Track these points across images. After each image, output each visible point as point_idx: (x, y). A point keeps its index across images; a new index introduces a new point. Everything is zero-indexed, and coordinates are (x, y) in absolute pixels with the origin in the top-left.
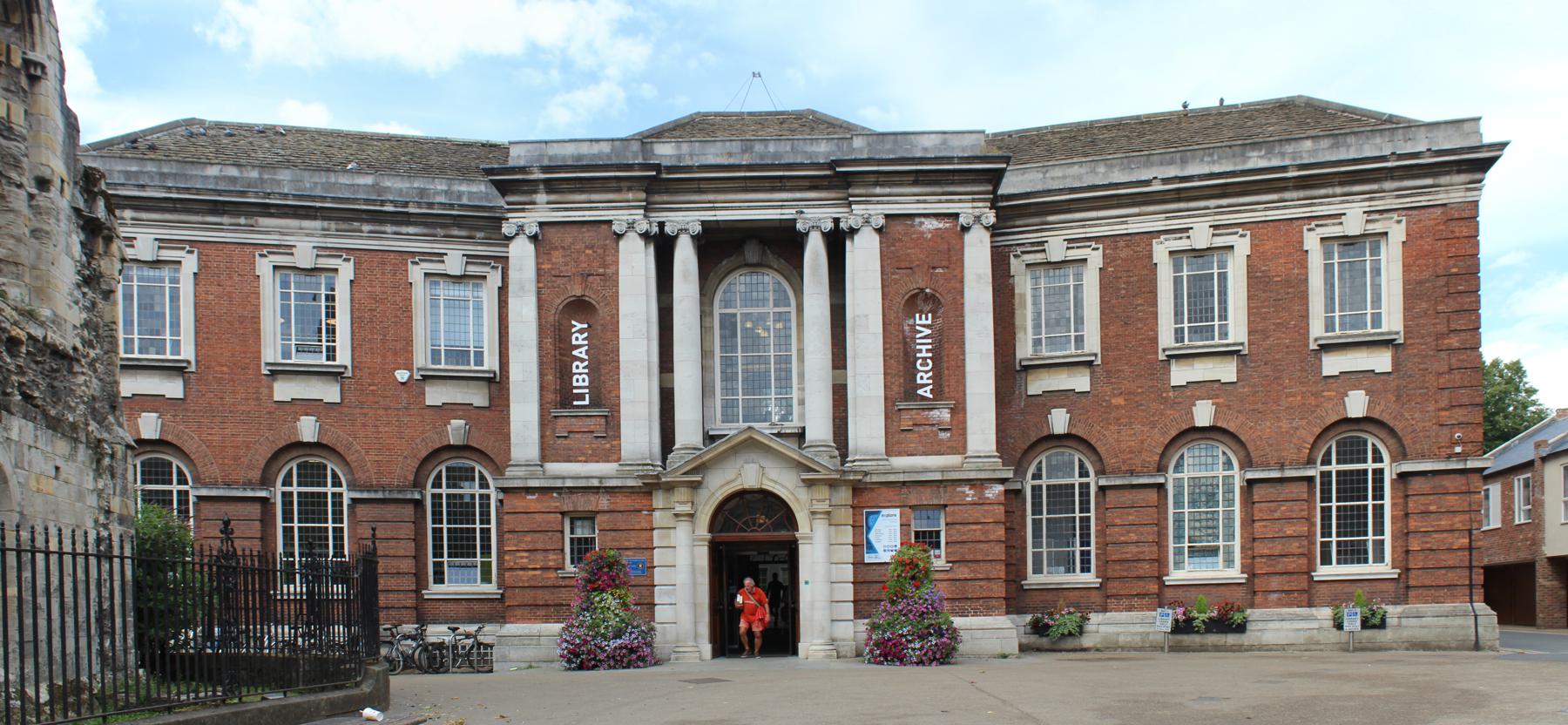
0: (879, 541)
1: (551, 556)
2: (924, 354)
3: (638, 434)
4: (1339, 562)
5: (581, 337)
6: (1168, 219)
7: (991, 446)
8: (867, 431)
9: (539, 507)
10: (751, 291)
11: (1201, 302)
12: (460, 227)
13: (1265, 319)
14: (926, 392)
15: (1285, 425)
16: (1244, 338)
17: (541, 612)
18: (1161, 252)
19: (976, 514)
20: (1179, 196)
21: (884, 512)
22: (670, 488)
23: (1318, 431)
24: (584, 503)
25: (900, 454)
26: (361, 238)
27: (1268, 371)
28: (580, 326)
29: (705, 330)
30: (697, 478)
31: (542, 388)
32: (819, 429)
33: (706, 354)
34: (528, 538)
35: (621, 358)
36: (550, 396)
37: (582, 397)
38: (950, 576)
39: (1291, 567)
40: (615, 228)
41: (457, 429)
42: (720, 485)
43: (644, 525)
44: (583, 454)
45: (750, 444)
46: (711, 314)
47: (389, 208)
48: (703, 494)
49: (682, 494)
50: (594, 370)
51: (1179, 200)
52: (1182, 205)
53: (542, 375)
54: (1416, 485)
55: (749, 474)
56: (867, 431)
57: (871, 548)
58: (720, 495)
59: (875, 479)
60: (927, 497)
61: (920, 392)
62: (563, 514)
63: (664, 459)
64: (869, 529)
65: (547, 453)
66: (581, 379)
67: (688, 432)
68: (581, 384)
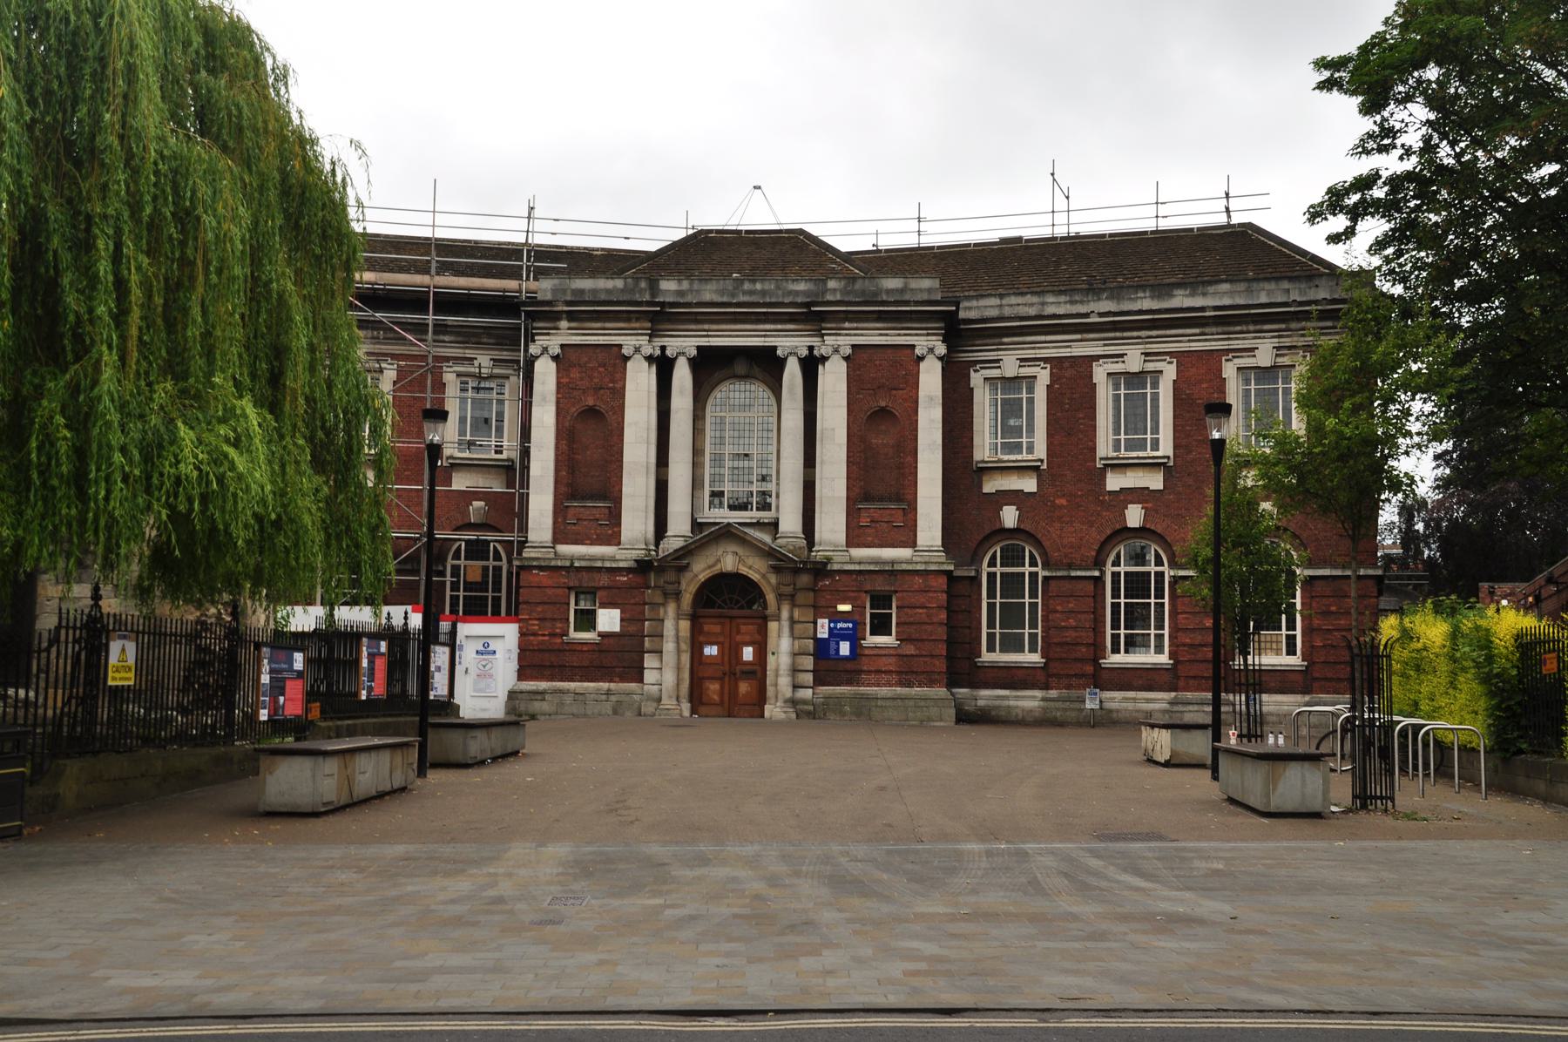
3: (636, 522)
9: (550, 582)
10: (738, 398)
11: (1135, 417)
16: (1170, 453)
17: (547, 672)
18: (1100, 373)
19: (922, 599)
20: (1114, 327)
24: (586, 581)
25: (858, 546)
31: (556, 482)
32: (790, 522)
34: (539, 609)
38: (900, 652)
42: (701, 569)
48: (688, 575)
49: (671, 576)
51: (1115, 330)
52: (1118, 334)
54: (1319, 585)
55: (728, 560)
56: (832, 526)
58: (702, 577)
60: (880, 585)
62: (570, 588)
63: (657, 545)
65: (560, 536)
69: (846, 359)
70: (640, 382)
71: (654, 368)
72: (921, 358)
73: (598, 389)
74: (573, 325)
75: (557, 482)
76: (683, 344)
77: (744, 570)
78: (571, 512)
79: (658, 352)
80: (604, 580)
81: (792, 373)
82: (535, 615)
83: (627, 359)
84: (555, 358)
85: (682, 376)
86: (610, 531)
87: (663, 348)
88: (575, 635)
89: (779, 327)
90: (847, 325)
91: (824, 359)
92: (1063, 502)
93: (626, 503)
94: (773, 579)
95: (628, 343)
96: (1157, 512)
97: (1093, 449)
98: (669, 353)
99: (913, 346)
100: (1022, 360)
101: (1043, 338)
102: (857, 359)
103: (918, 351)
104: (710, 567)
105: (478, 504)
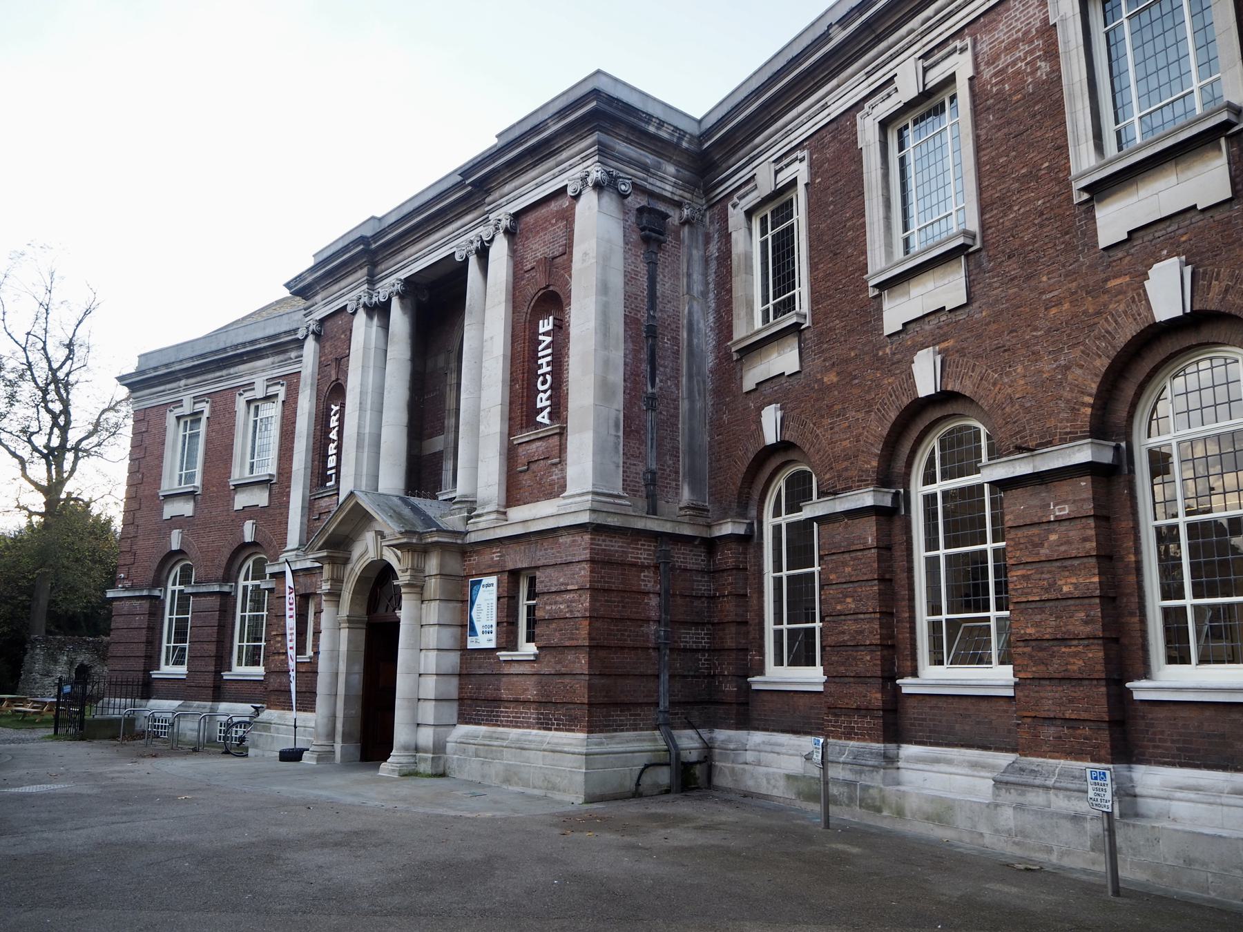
4: (1203, 660)
6: (869, 75)
13: (1003, 176)
15: (1047, 366)
23: (1102, 364)
26: (290, 364)
27: (1012, 268)
36: (315, 481)
39: (1076, 665)
71: (376, 319)
92: (831, 378)
96: (962, 352)
97: (864, 268)
99: (563, 190)
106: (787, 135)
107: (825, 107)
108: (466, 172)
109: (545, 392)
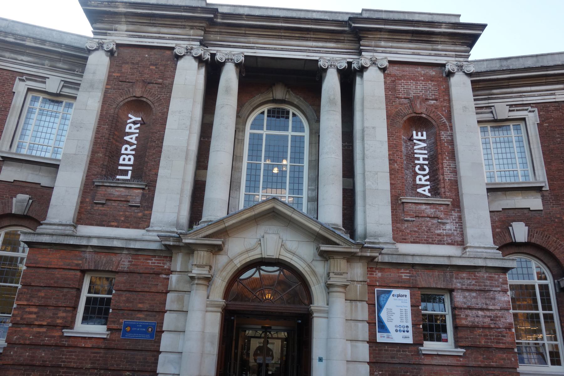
0: (391, 320)
1: (61, 314)
2: (421, 162)
3: (169, 206)
5: (134, 127)
7: (489, 241)
8: (376, 217)
9: (61, 264)
12: (64, 62)
14: (425, 191)
21: (395, 292)
22: (190, 249)
25: (404, 241)
28: (134, 119)
29: (238, 141)
30: (219, 242)
32: (331, 213)
33: (236, 158)
35: (165, 143)
37: (125, 173)
40: (176, 51)
41: (22, 201)
43: (160, 288)
44: (116, 220)
45: (273, 215)
46: (244, 131)
47: (11, 39)
48: (222, 259)
49: (202, 256)
50: (139, 155)
53: (94, 152)
57: (383, 328)
58: (238, 263)
59: (387, 259)
61: (420, 190)
64: (380, 308)
65: (84, 215)
66: (127, 158)
67: (215, 207)
68: (126, 162)
69: (383, 70)
70: (189, 78)
71: (203, 71)
72: (450, 74)
73: (146, 83)
74: (131, 27)
75: (92, 162)
76: (231, 53)
77: (287, 257)
78: (101, 190)
79: (207, 57)
80: (125, 263)
81: (331, 85)
82: (35, 301)
83: (178, 57)
84: (111, 53)
85: (229, 78)
86: (140, 215)
87: (213, 55)
88: (83, 329)
89: (320, 44)
90: (383, 43)
91: (363, 69)
93: (161, 184)
94: (320, 268)
95: (180, 47)
98: (218, 57)
99: (444, 65)
100: (511, 106)
101: (528, 89)
102: (392, 71)
103: (448, 68)
104: (247, 251)
105: (20, 197)
106: (521, 97)
107: (554, 94)
108: (355, 18)
109: (424, 175)
